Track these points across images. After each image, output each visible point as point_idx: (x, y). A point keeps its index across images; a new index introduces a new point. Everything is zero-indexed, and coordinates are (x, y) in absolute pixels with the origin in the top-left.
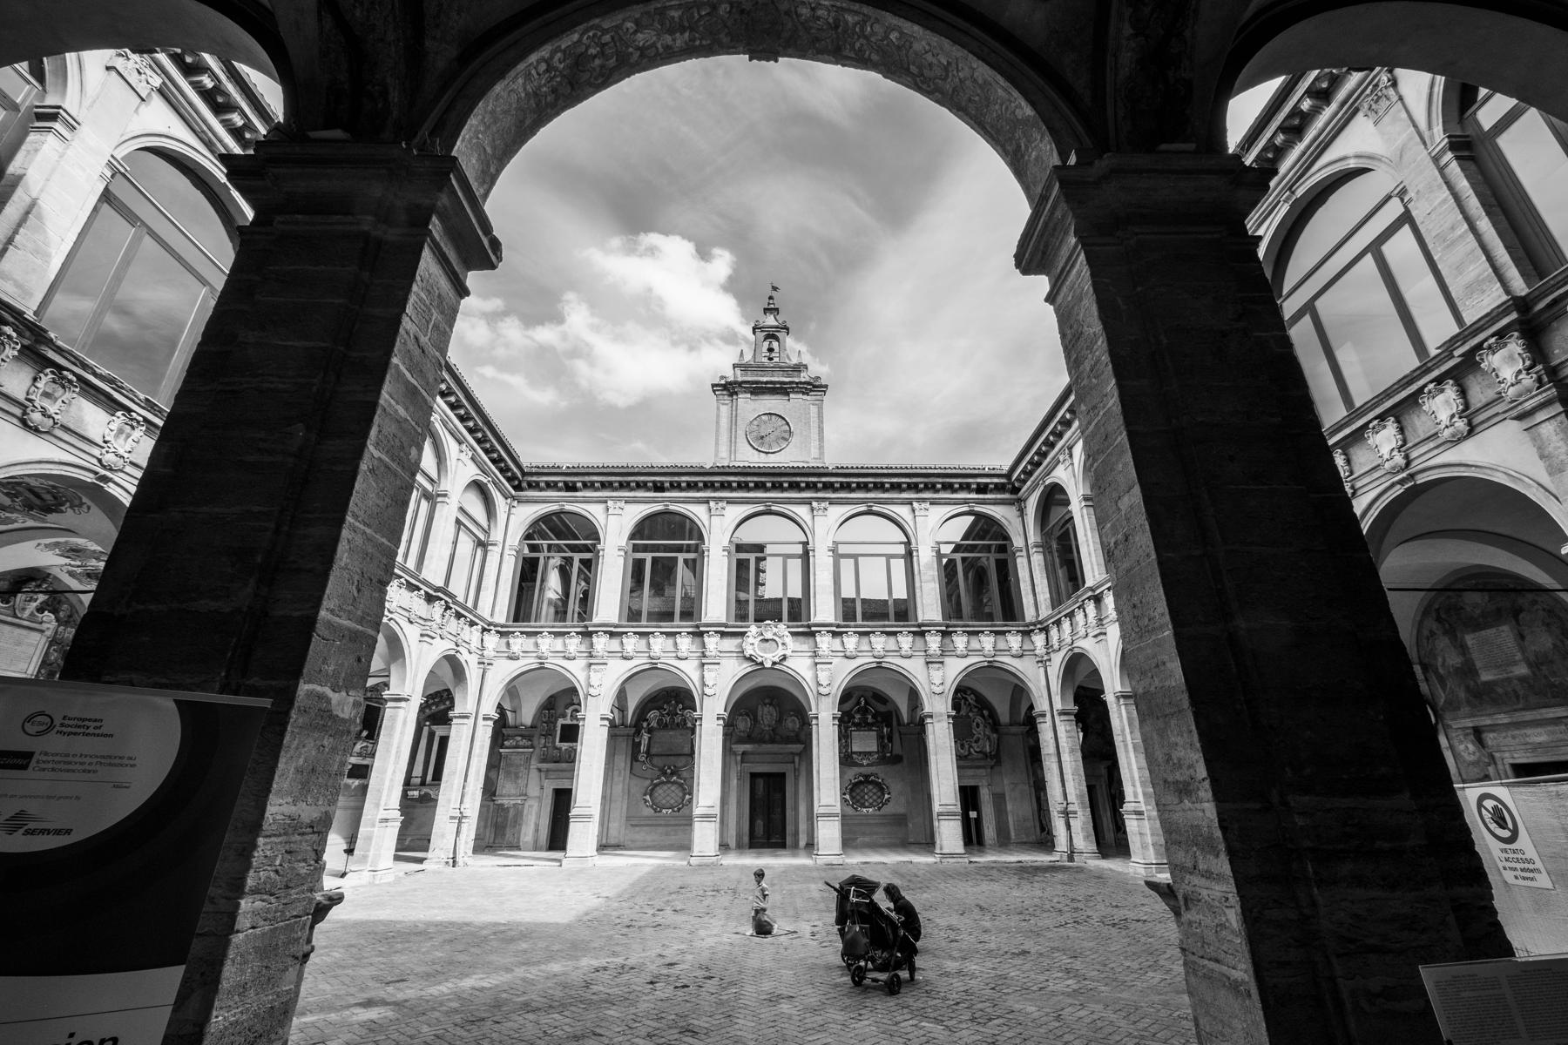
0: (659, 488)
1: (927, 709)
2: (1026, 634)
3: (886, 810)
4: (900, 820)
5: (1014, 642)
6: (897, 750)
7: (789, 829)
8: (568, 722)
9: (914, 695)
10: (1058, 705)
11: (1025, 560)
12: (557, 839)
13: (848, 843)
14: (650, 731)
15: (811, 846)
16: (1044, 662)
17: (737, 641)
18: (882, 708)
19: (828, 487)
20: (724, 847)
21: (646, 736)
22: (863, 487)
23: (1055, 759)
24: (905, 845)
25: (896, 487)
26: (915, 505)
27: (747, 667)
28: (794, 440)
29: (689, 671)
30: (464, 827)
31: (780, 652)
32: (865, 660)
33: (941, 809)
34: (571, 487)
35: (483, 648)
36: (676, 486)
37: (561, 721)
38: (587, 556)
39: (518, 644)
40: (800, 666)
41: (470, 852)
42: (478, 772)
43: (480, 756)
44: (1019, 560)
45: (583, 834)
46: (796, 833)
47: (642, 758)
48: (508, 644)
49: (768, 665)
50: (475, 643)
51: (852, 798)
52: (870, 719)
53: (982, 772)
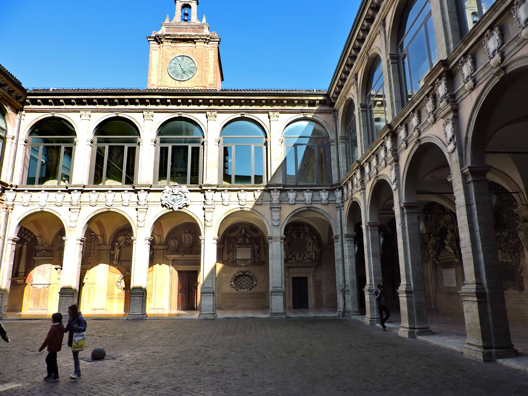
0: (111, 102)
2: (332, 191)
3: (254, 290)
5: (324, 195)
10: (345, 232)
11: (335, 147)
14: (120, 248)
16: (340, 207)
17: (160, 194)
18: (254, 235)
19: (217, 102)
21: (117, 251)
22: (238, 102)
23: (341, 262)
25: (259, 103)
26: (271, 113)
27: (165, 210)
28: (198, 73)
29: (130, 214)
31: (184, 201)
33: (274, 289)
34: (57, 102)
36: (122, 102)
38: (68, 145)
39: (26, 196)
40: (195, 211)
44: (332, 147)
52: (247, 241)
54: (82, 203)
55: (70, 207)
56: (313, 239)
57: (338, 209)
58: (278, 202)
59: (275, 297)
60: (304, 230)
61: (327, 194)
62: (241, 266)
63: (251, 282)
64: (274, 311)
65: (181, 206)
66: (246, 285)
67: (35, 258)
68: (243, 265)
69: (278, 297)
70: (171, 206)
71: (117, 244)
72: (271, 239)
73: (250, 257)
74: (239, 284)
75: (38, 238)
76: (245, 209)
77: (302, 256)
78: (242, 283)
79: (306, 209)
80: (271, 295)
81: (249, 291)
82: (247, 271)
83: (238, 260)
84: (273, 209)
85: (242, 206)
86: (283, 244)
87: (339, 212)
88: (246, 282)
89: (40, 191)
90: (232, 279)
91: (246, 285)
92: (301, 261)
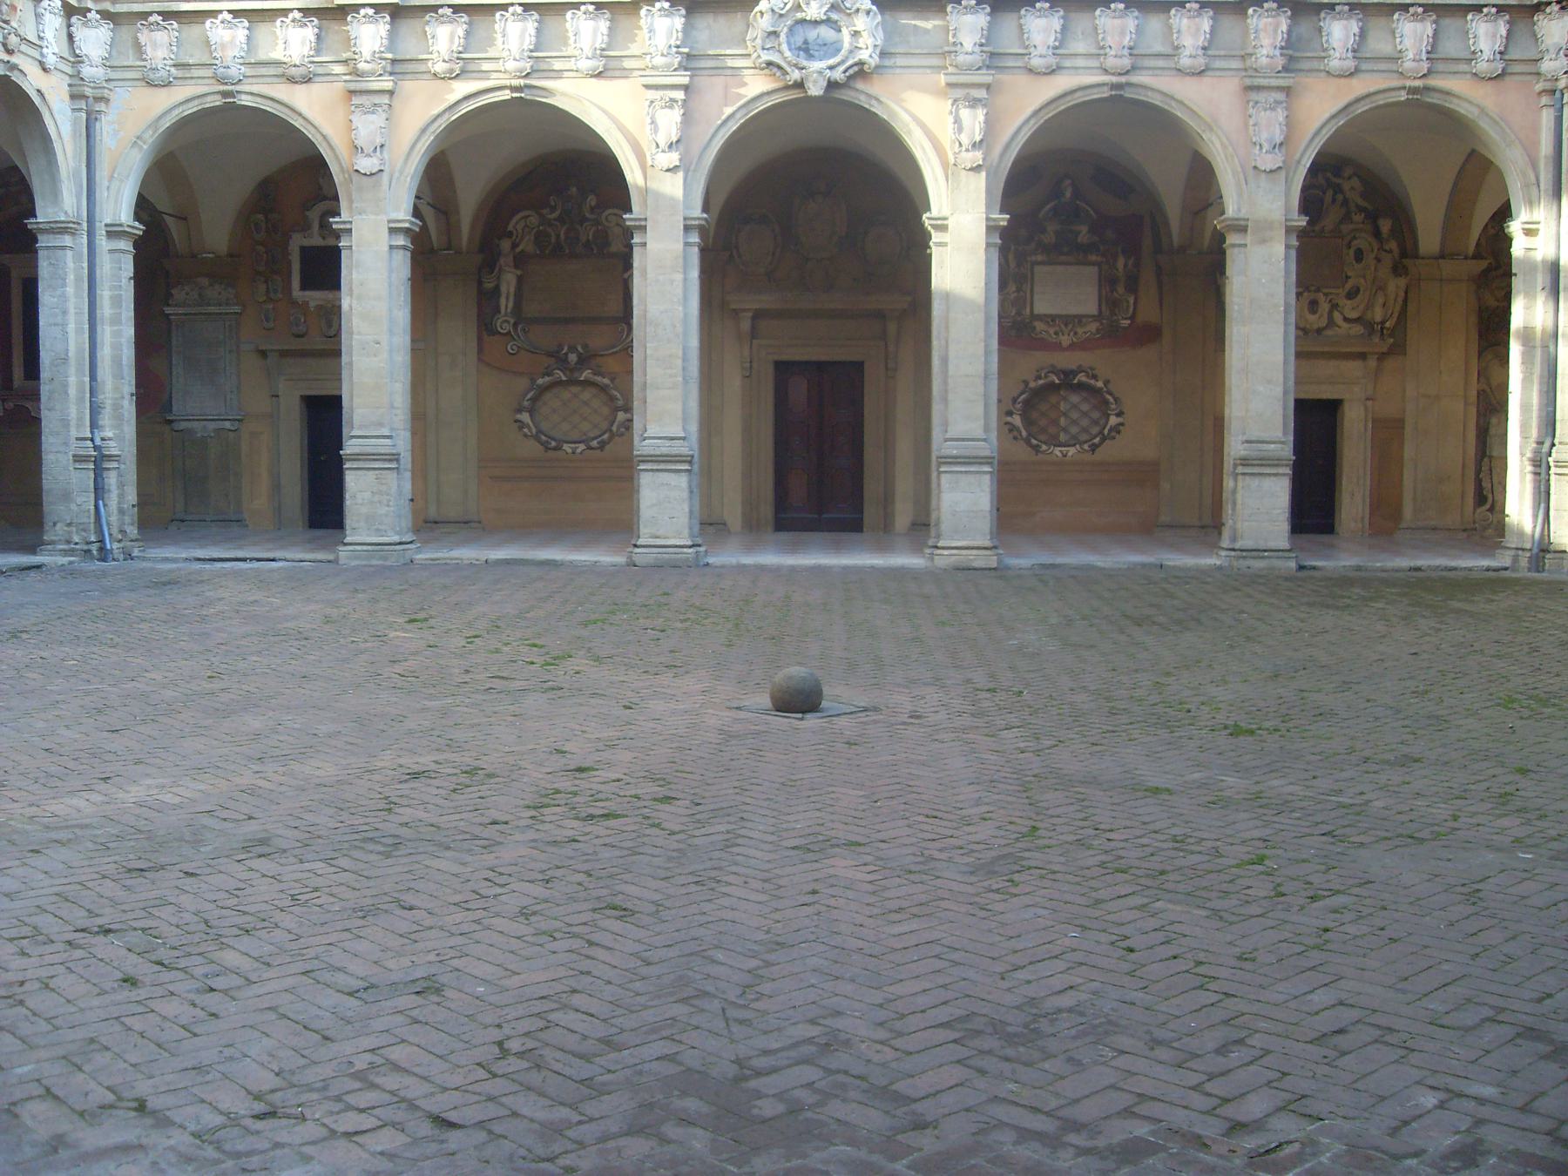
1: (1232, 206)
3: (1111, 451)
4: (1143, 474)
5: (1486, 35)
6: (1148, 311)
7: (872, 488)
8: (316, 241)
9: (1201, 175)
12: (324, 508)
13: (1012, 516)
14: (520, 261)
15: (922, 527)
20: (710, 526)
24: (1149, 528)
30: (111, 480)
32: (1081, 78)
35: (77, 59)
37: (297, 241)
41: (133, 531)
42: (117, 360)
43: (116, 320)
45: (374, 498)
46: (887, 500)
47: (503, 323)
48: (138, 48)
49: (815, 89)
50: (54, 47)
51: (1028, 422)
52: (1083, 233)
53: (1353, 368)
54: (399, 68)
55: (352, 86)
56: (1377, 234)
57: (1545, 100)
58: (1280, 62)
59: (1254, 483)
60: (1338, 189)
61: (1503, 30)
62: (1057, 347)
63: (1096, 415)
64: (1245, 543)
65: (838, 75)
66: (1074, 430)
67: (168, 310)
68: (1065, 340)
69: (1267, 483)
70: (796, 75)
71: (505, 245)
72: (1243, 229)
73: (1091, 308)
74: (1043, 422)
75: (169, 221)
76: (1128, 94)
77: (1324, 307)
78: (1055, 422)
79: (1403, 96)
80: (1236, 475)
81: (1088, 457)
82: (1080, 370)
83: (1041, 318)
84: (1254, 96)
85: (1114, 79)
86: (1293, 253)
87: (1547, 117)
88: (1074, 415)
89: (213, 14)
90: (1014, 400)
91: (1074, 430)
92: (1319, 331)
